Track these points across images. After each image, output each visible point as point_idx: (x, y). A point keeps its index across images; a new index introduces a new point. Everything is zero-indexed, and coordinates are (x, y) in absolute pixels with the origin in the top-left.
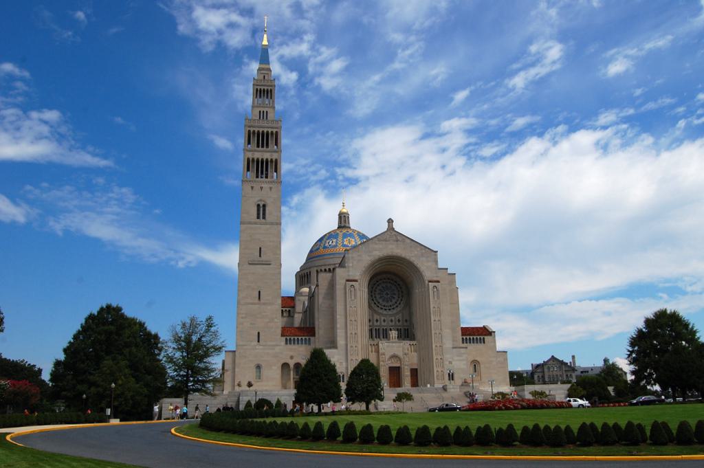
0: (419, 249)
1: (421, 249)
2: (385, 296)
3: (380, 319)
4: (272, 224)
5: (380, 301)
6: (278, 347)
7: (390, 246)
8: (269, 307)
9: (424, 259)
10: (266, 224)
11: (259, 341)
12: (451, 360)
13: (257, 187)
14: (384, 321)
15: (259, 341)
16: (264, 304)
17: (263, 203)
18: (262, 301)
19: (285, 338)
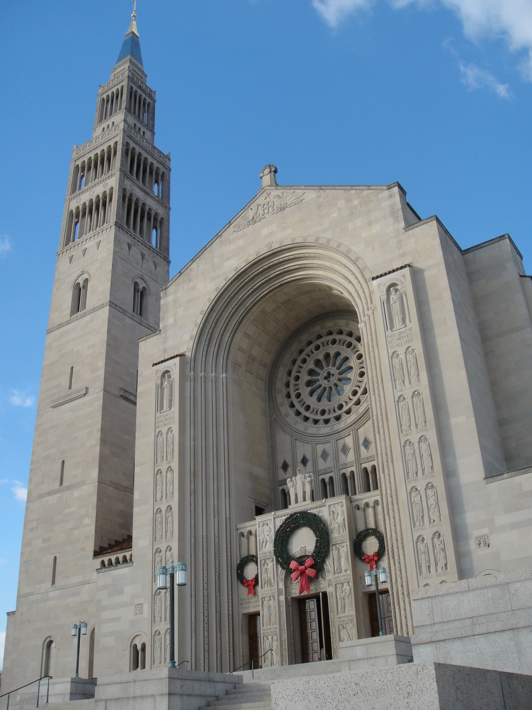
0: (341, 203)
1: (348, 200)
2: (324, 383)
3: (314, 451)
4: (94, 310)
5: (312, 401)
6: (87, 587)
7: (265, 232)
8: (76, 493)
9: (359, 222)
10: (85, 315)
11: (53, 582)
12: (485, 531)
13: (76, 252)
14: (325, 455)
15: (53, 582)
16: (69, 488)
17: (85, 276)
18: (65, 483)
19: (99, 561)
